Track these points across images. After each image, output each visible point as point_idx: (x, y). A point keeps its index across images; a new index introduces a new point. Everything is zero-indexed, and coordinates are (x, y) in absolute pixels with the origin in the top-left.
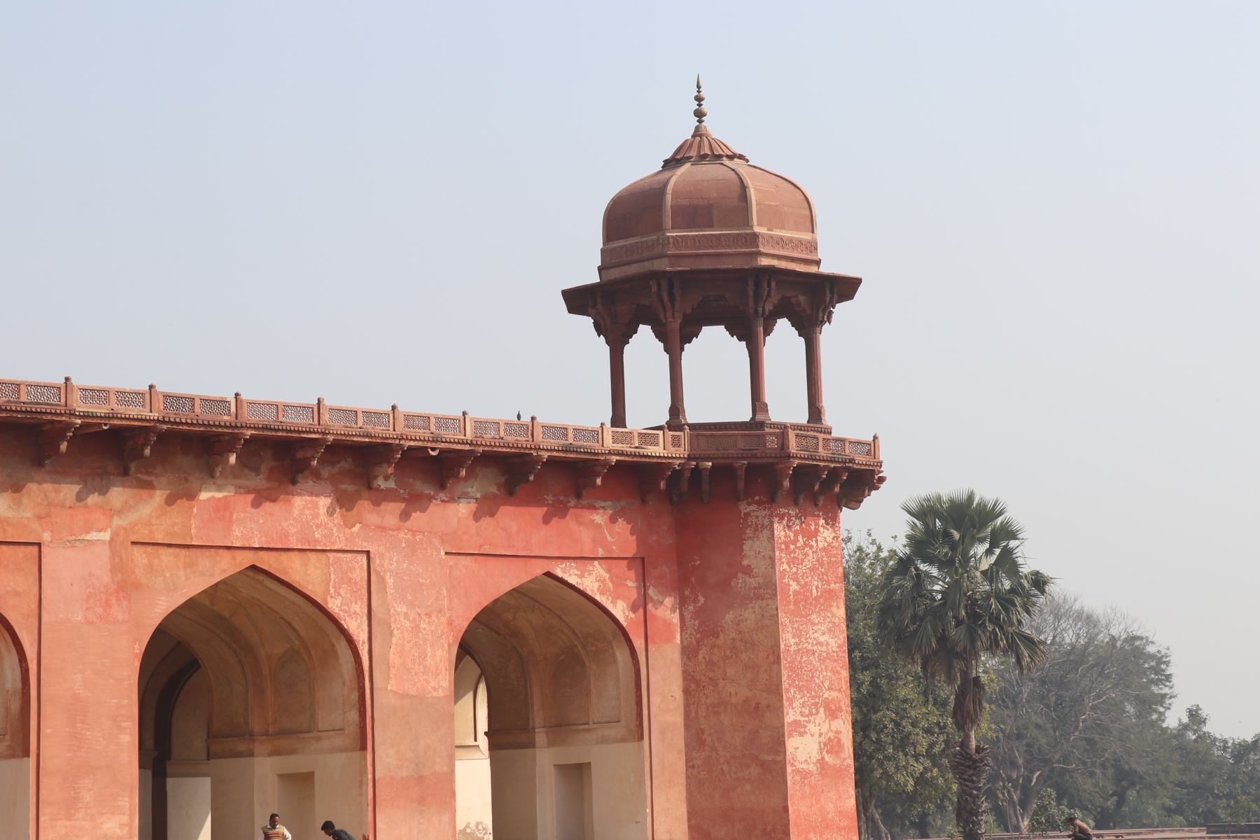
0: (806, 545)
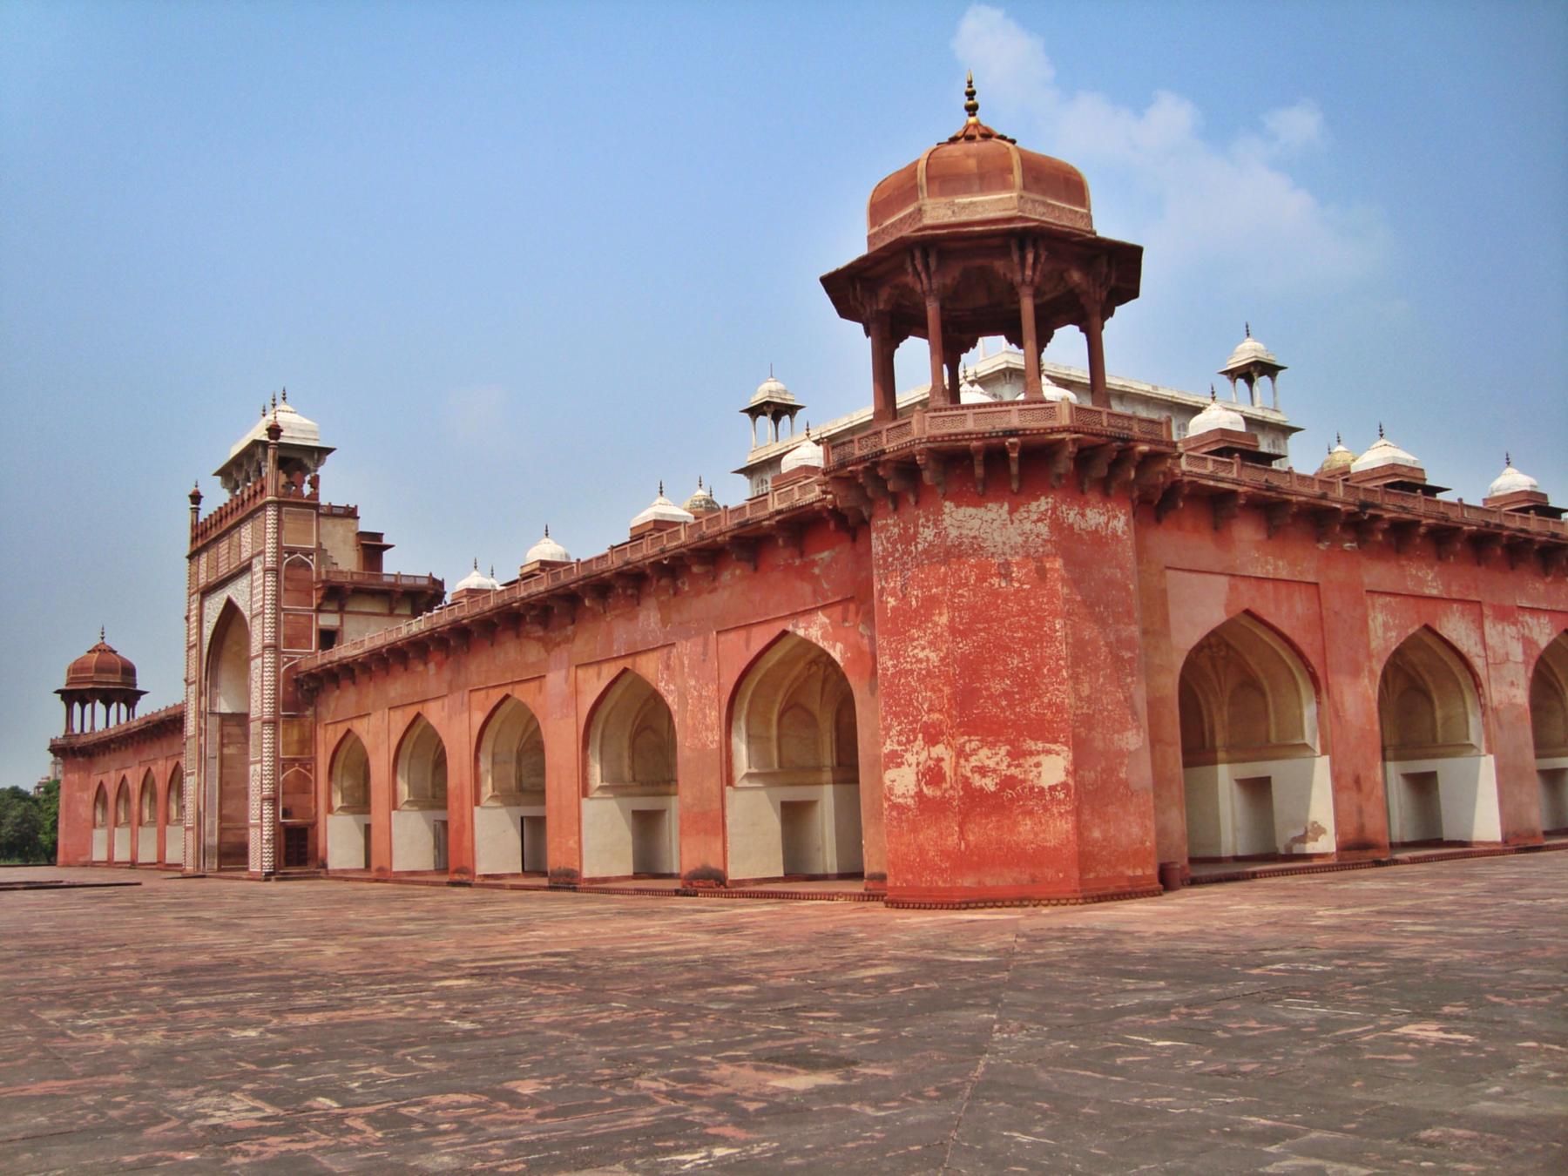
0: (904, 553)
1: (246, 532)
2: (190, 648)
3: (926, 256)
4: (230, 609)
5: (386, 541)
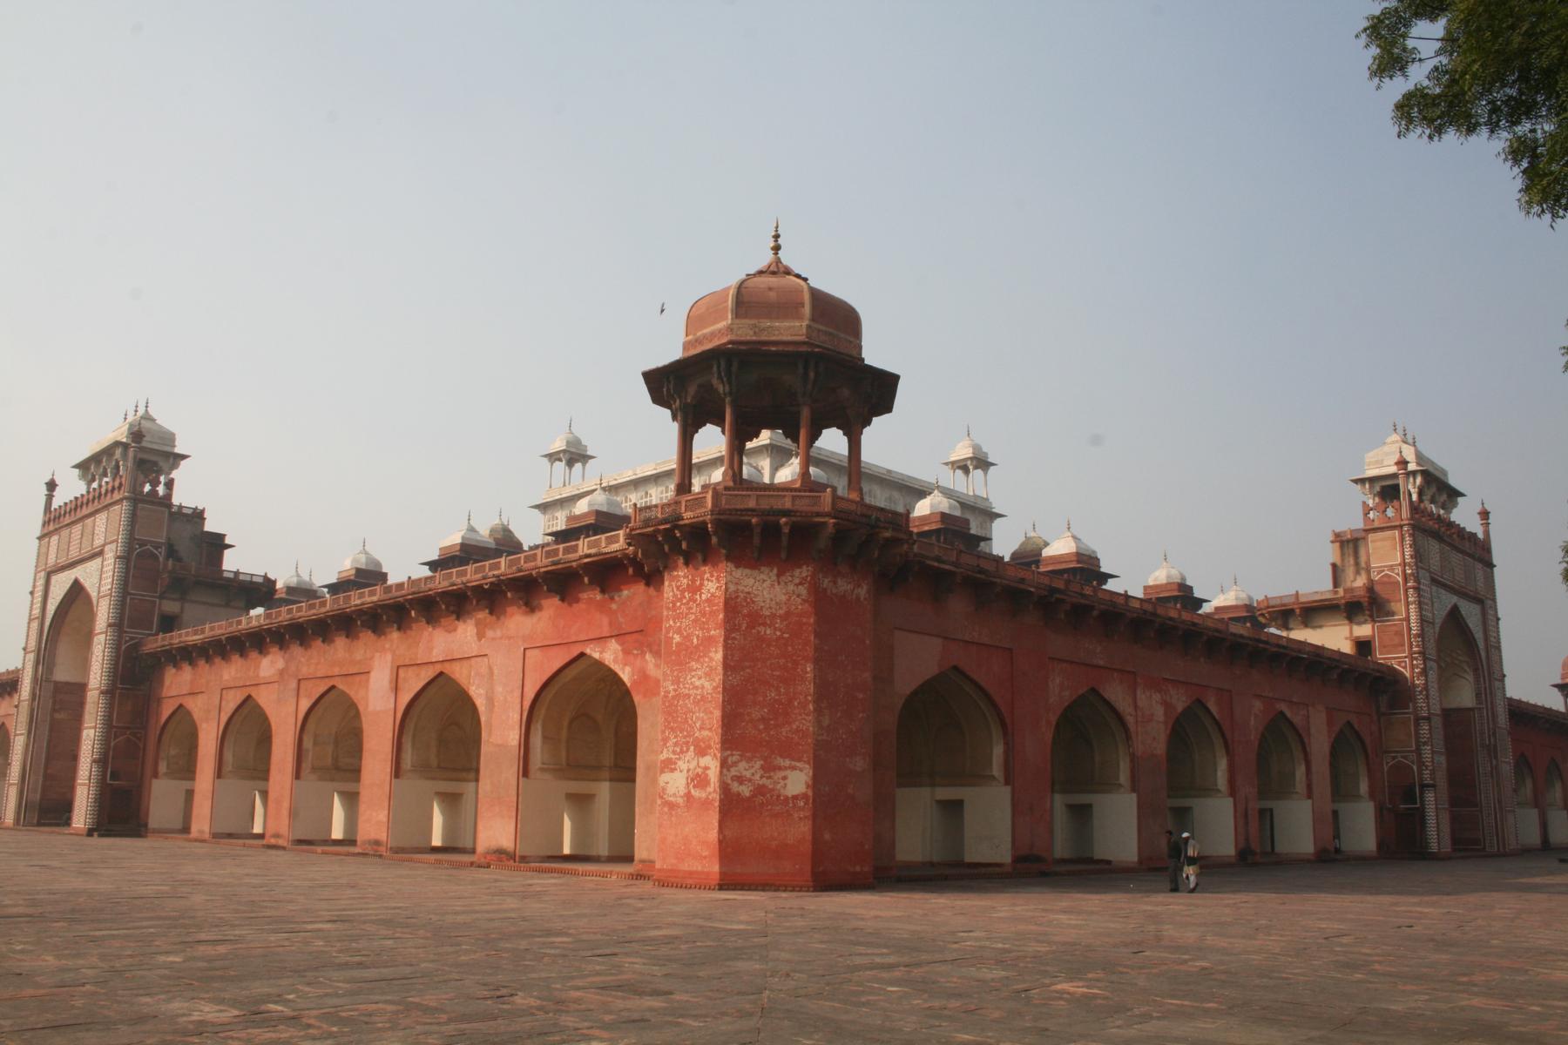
1: (101, 519)
2: (30, 620)
3: (729, 365)
4: (77, 589)
5: (227, 541)
